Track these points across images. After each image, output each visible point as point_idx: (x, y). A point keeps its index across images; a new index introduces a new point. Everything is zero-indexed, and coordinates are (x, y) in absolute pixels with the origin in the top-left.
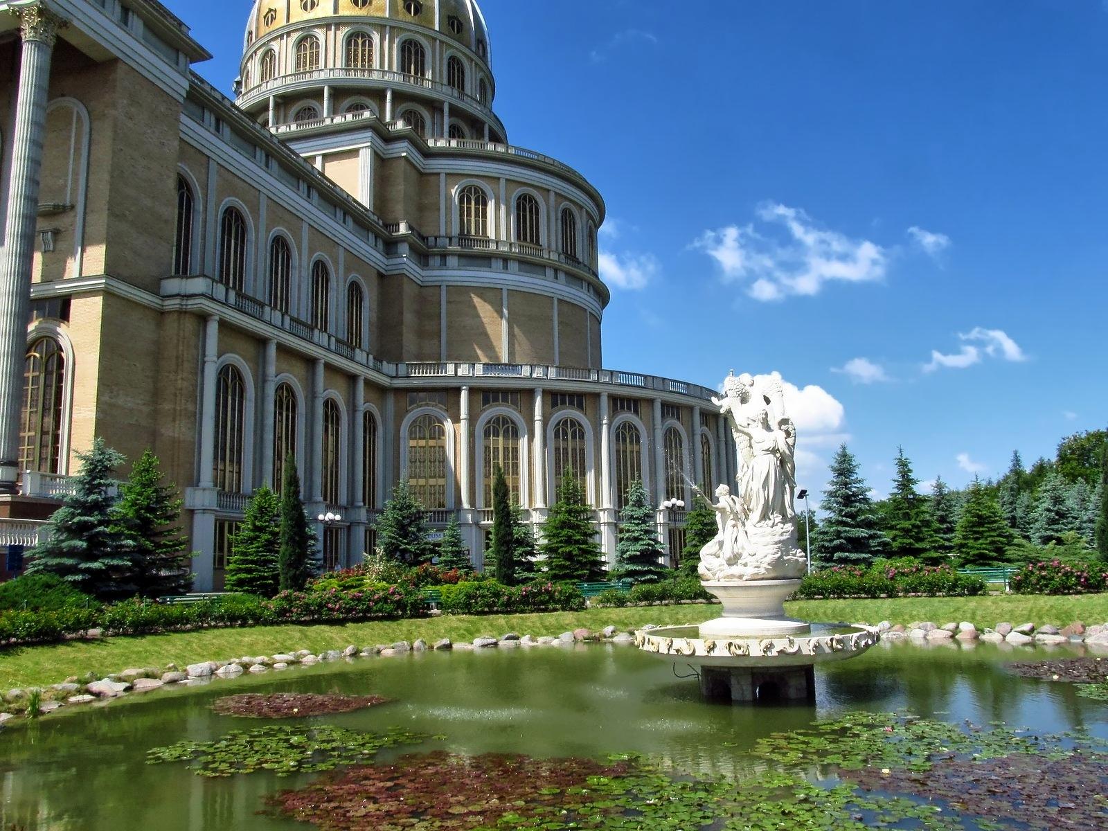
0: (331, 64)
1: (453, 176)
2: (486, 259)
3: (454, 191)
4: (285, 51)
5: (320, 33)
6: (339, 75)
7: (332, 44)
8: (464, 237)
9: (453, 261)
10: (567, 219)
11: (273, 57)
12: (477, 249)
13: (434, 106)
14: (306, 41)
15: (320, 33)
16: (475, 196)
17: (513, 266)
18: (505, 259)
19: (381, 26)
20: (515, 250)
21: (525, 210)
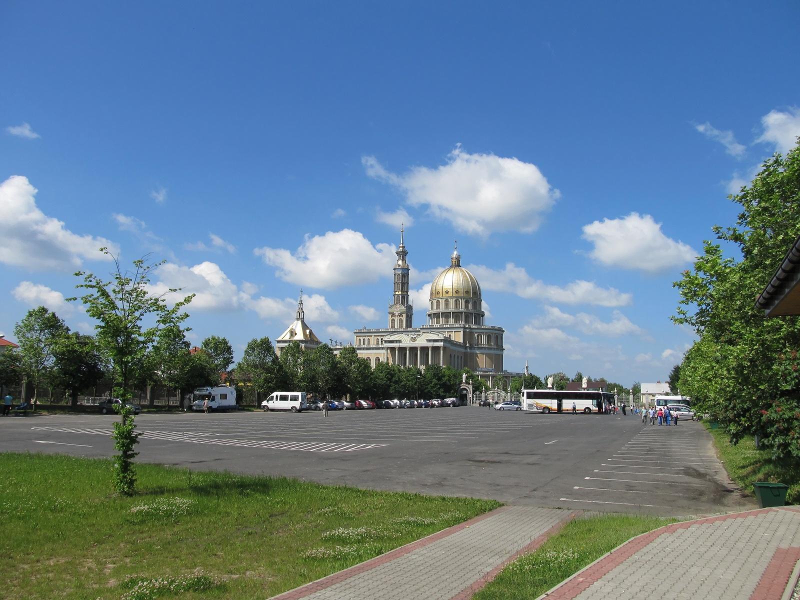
0: (452, 308)
1: (476, 333)
2: (482, 348)
3: (476, 335)
4: (442, 302)
5: (449, 299)
6: (453, 310)
7: (452, 302)
8: (478, 345)
9: (476, 349)
10: (497, 337)
11: (439, 302)
12: (480, 346)
13: (471, 314)
14: (447, 303)
15: (449, 299)
16: (480, 335)
17: (486, 349)
18: (485, 348)
19: (461, 298)
20: (487, 346)
21: (489, 338)
